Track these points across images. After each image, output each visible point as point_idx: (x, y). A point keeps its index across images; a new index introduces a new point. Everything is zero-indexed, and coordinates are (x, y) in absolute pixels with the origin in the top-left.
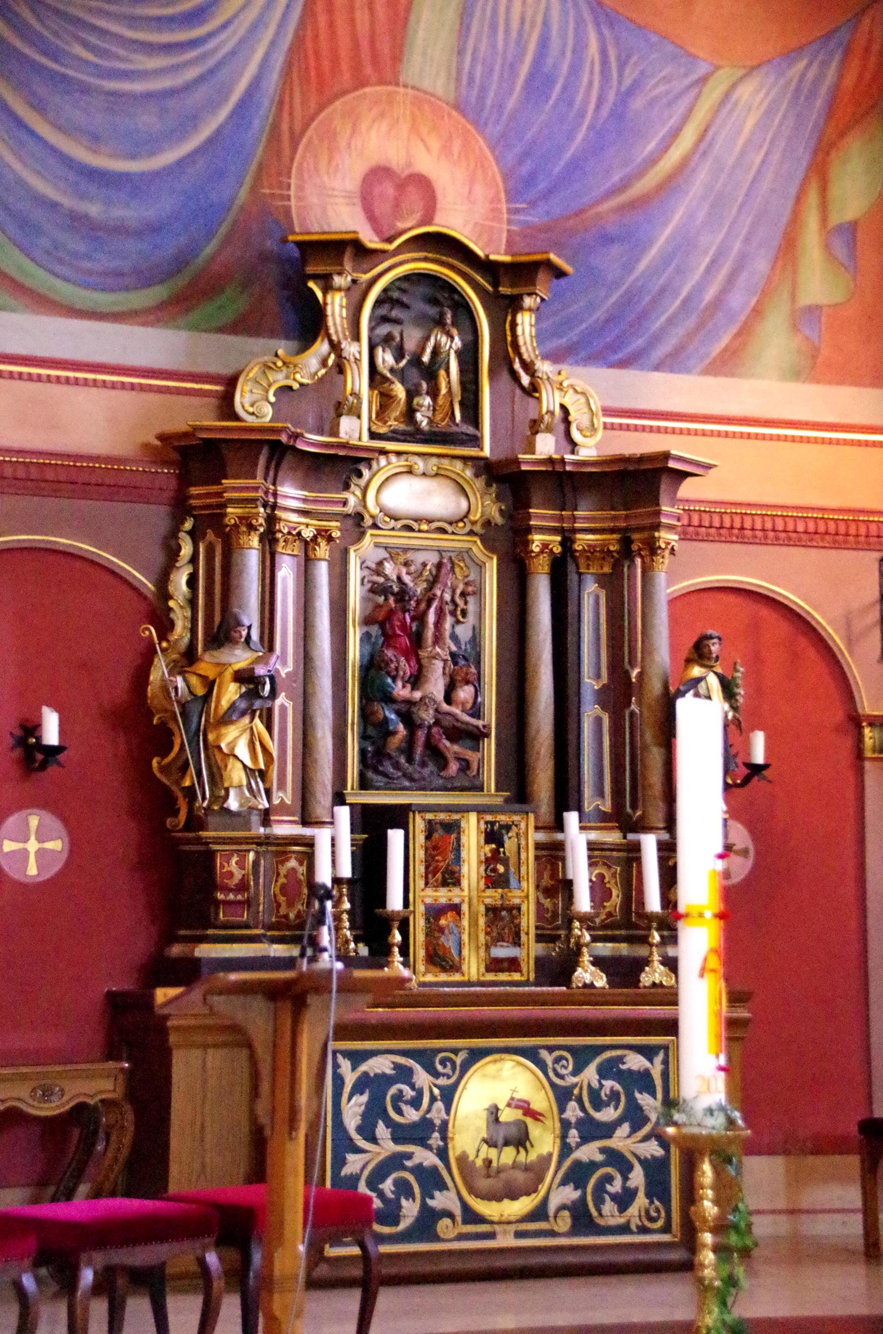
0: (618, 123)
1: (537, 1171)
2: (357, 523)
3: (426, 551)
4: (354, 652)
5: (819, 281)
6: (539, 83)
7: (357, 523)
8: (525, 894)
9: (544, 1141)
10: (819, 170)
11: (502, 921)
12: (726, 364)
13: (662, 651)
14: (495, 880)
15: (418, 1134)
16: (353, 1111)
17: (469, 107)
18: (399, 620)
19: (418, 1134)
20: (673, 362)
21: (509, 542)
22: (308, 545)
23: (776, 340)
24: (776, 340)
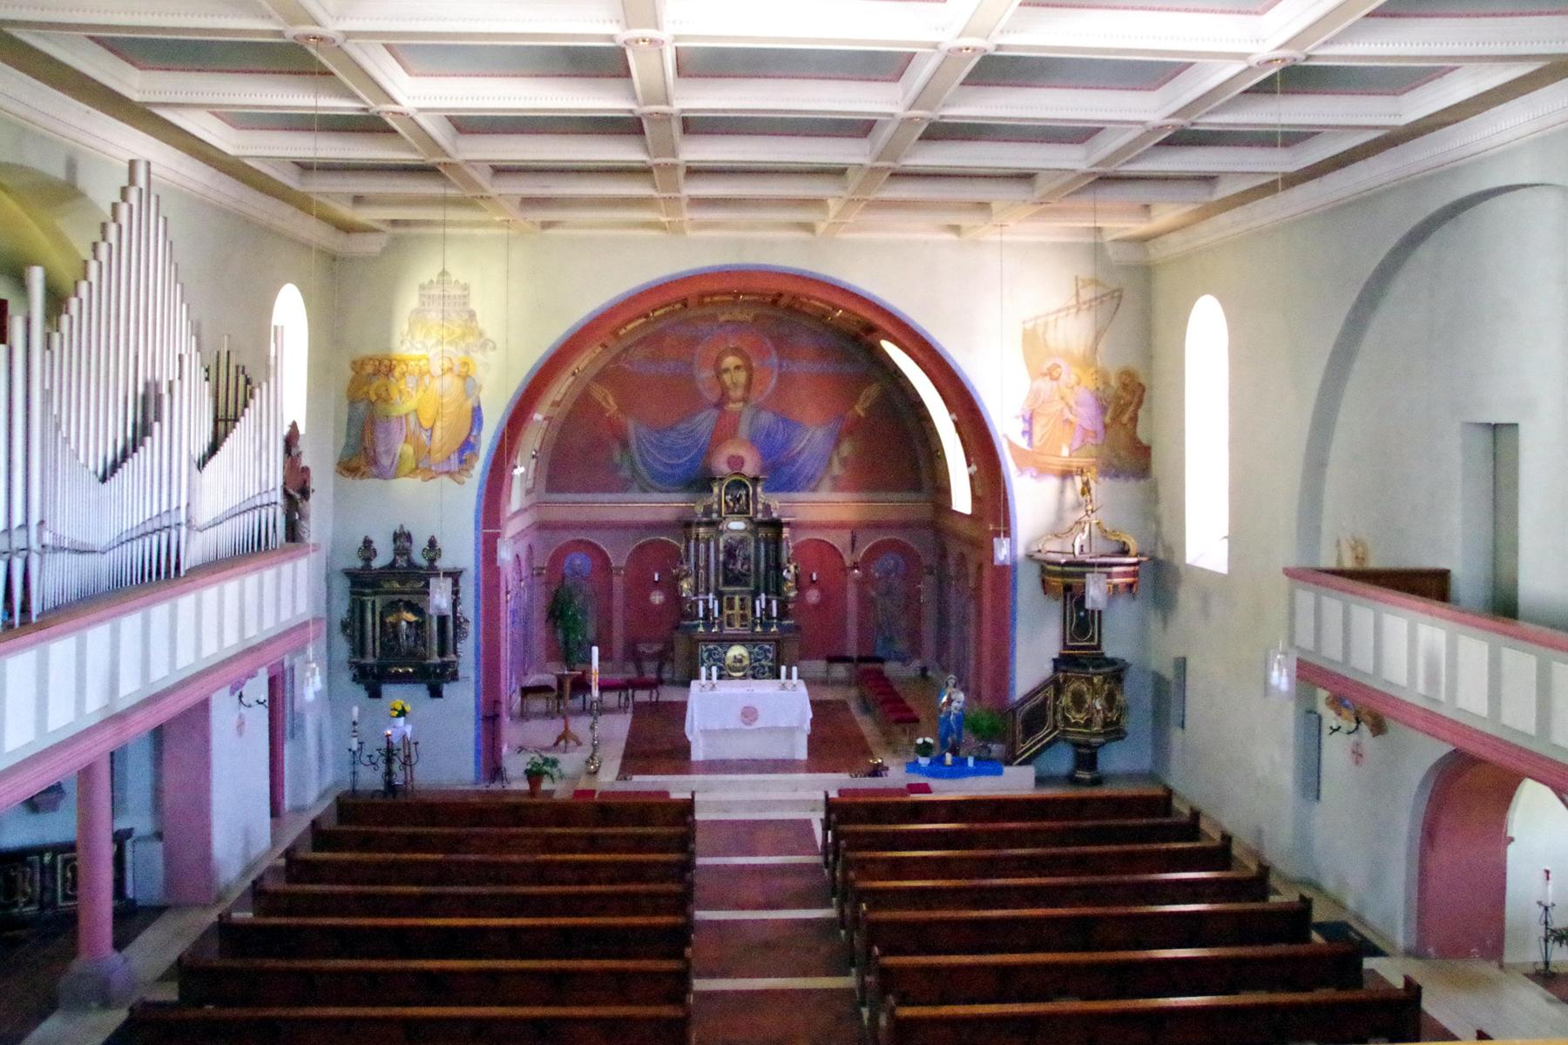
0: (788, 440)
1: (744, 669)
2: (721, 532)
3: (738, 536)
4: (721, 558)
5: (837, 469)
6: (768, 435)
7: (721, 532)
8: (749, 612)
9: (746, 662)
10: (837, 444)
11: (743, 617)
12: (814, 490)
13: (784, 560)
14: (742, 608)
15: (719, 660)
16: (705, 655)
17: (753, 441)
18: (731, 552)
19: (719, 660)
20: (803, 489)
21: (754, 532)
22: (707, 542)
23: (827, 483)
24: (827, 483)
